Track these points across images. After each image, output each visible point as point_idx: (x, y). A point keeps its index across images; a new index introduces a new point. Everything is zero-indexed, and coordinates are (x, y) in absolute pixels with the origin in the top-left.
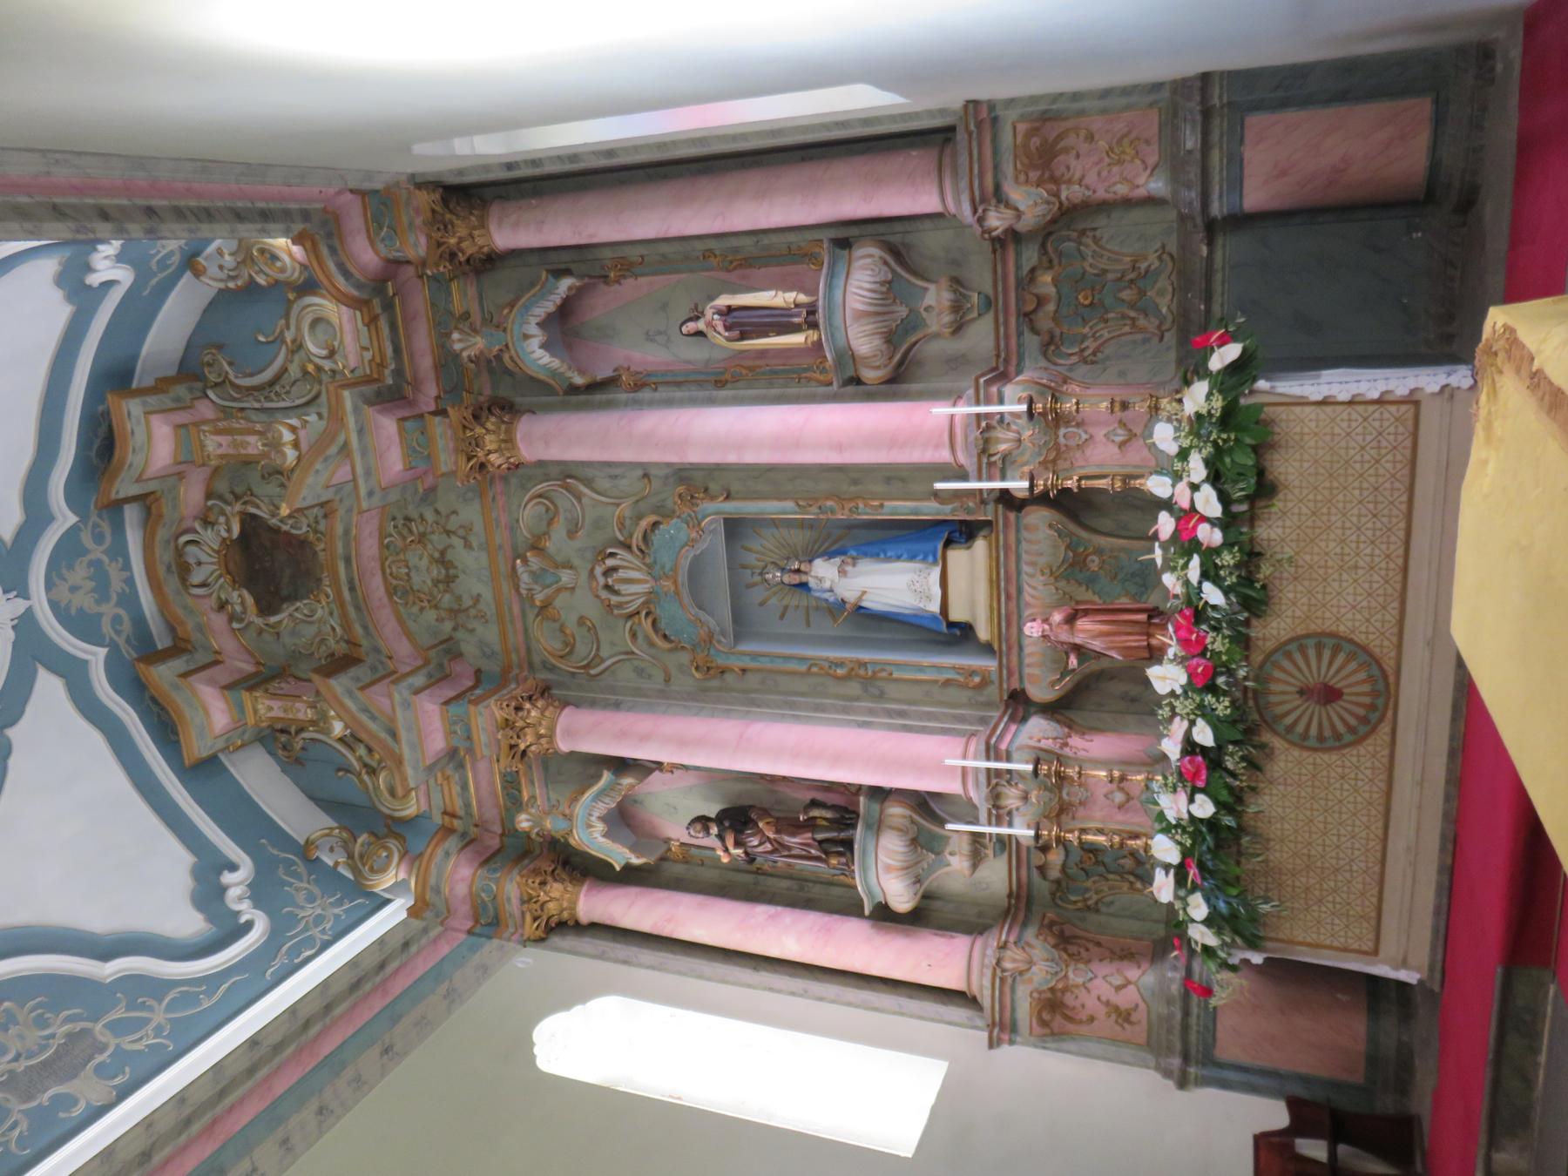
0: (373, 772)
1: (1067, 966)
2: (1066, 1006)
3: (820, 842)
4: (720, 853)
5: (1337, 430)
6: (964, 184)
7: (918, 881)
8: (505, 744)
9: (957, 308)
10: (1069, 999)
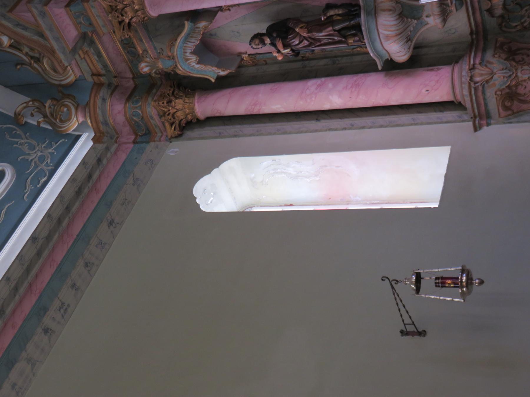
0: (38, 60)
1: (516, 70)
2: (519, 94)
3: (339, 31)
4: (276, 54)
7: (409, 39)
8: (115, 22)
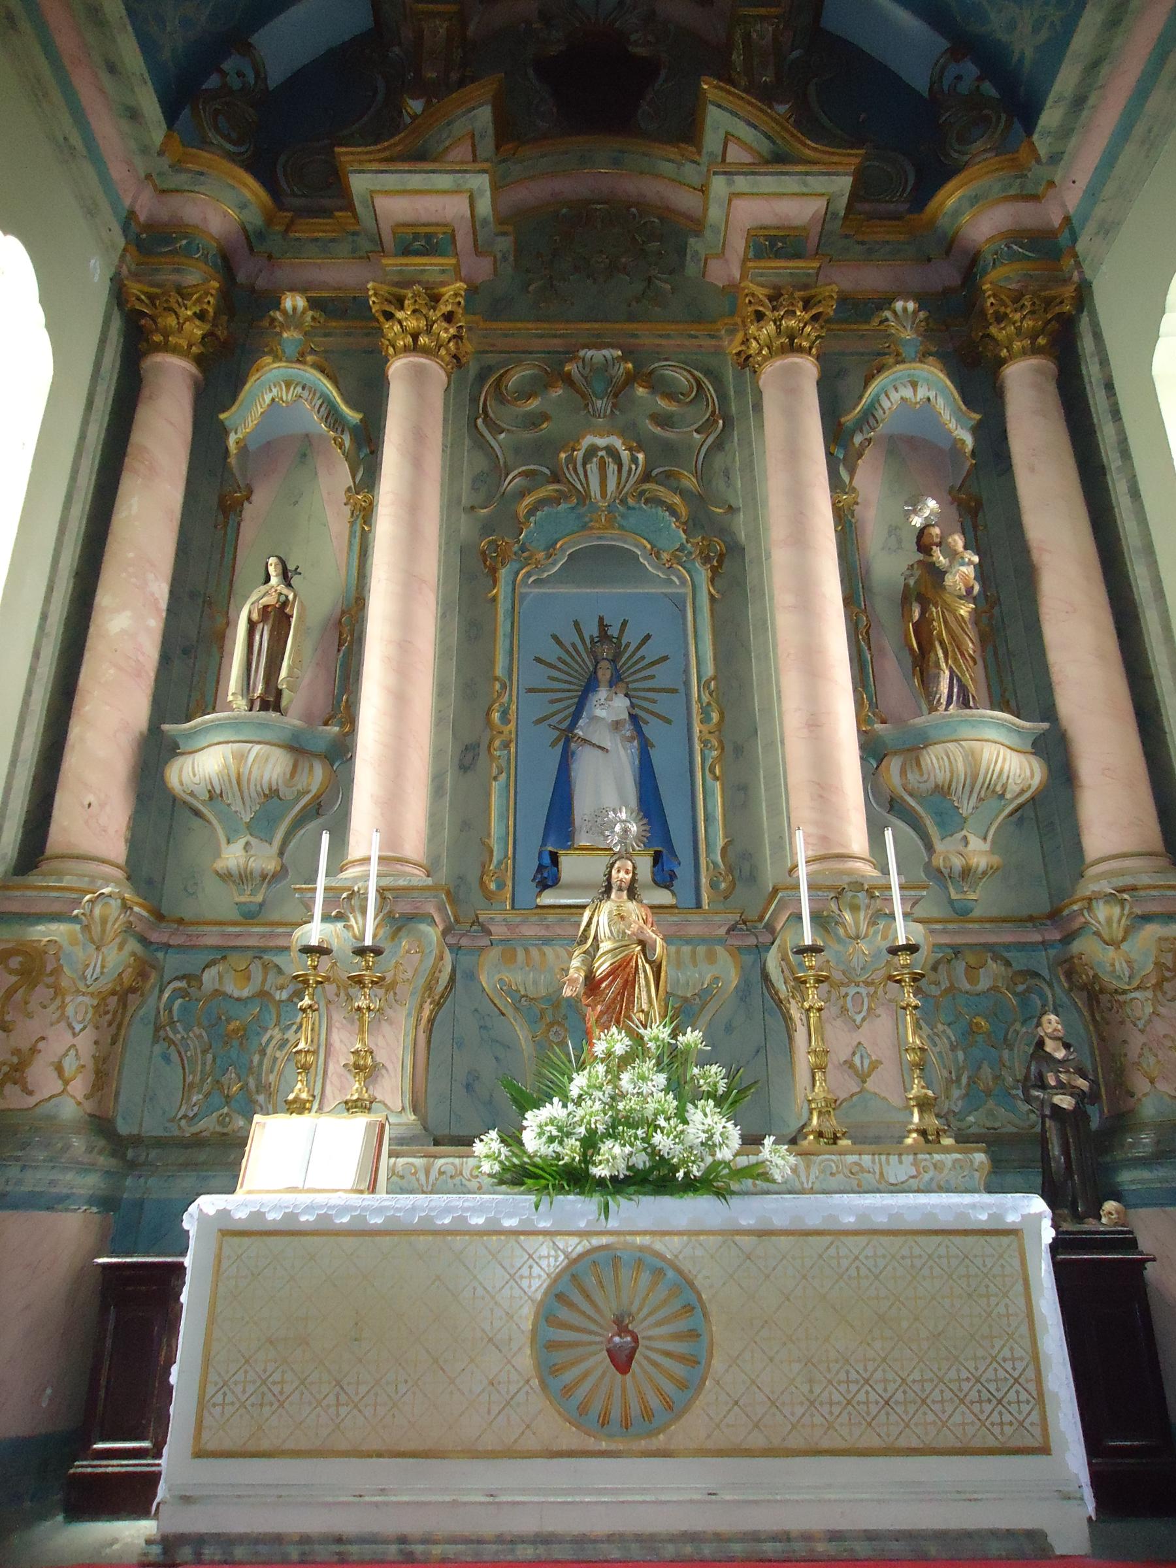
1: (92, 994)
5: (998, 1344)
6: (1145, 880)
9: (966, 873)
10: (41, 993)
